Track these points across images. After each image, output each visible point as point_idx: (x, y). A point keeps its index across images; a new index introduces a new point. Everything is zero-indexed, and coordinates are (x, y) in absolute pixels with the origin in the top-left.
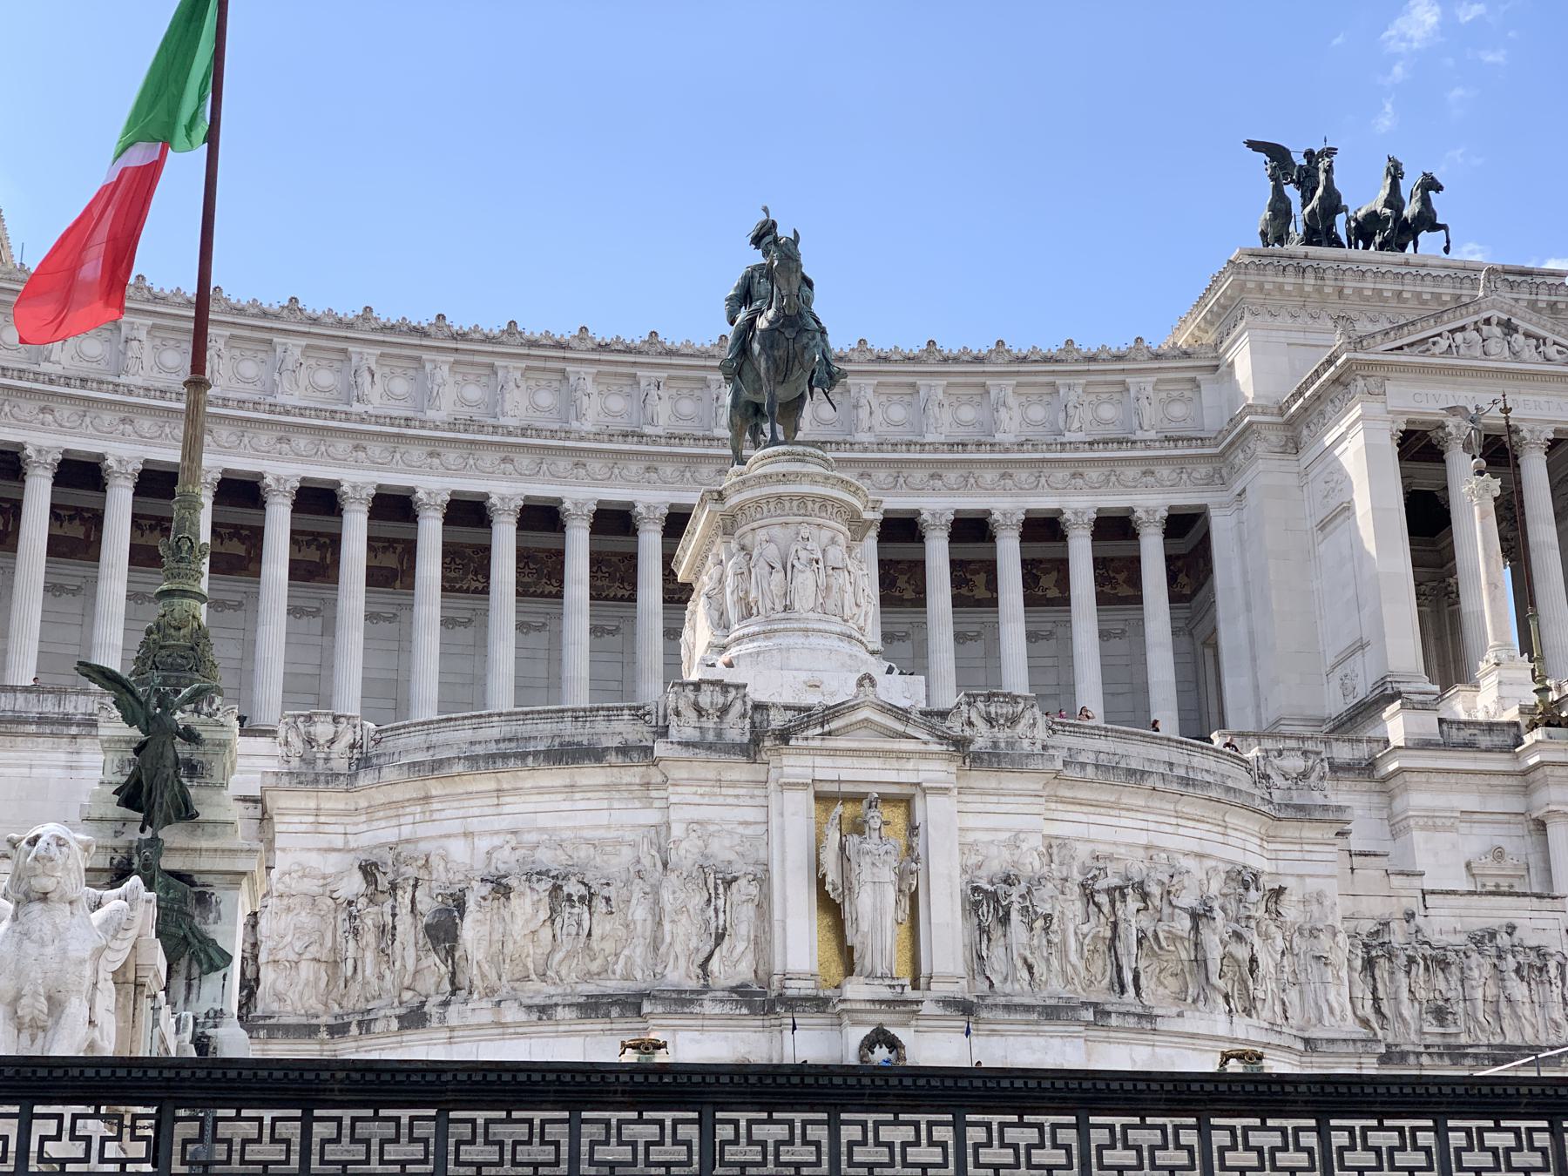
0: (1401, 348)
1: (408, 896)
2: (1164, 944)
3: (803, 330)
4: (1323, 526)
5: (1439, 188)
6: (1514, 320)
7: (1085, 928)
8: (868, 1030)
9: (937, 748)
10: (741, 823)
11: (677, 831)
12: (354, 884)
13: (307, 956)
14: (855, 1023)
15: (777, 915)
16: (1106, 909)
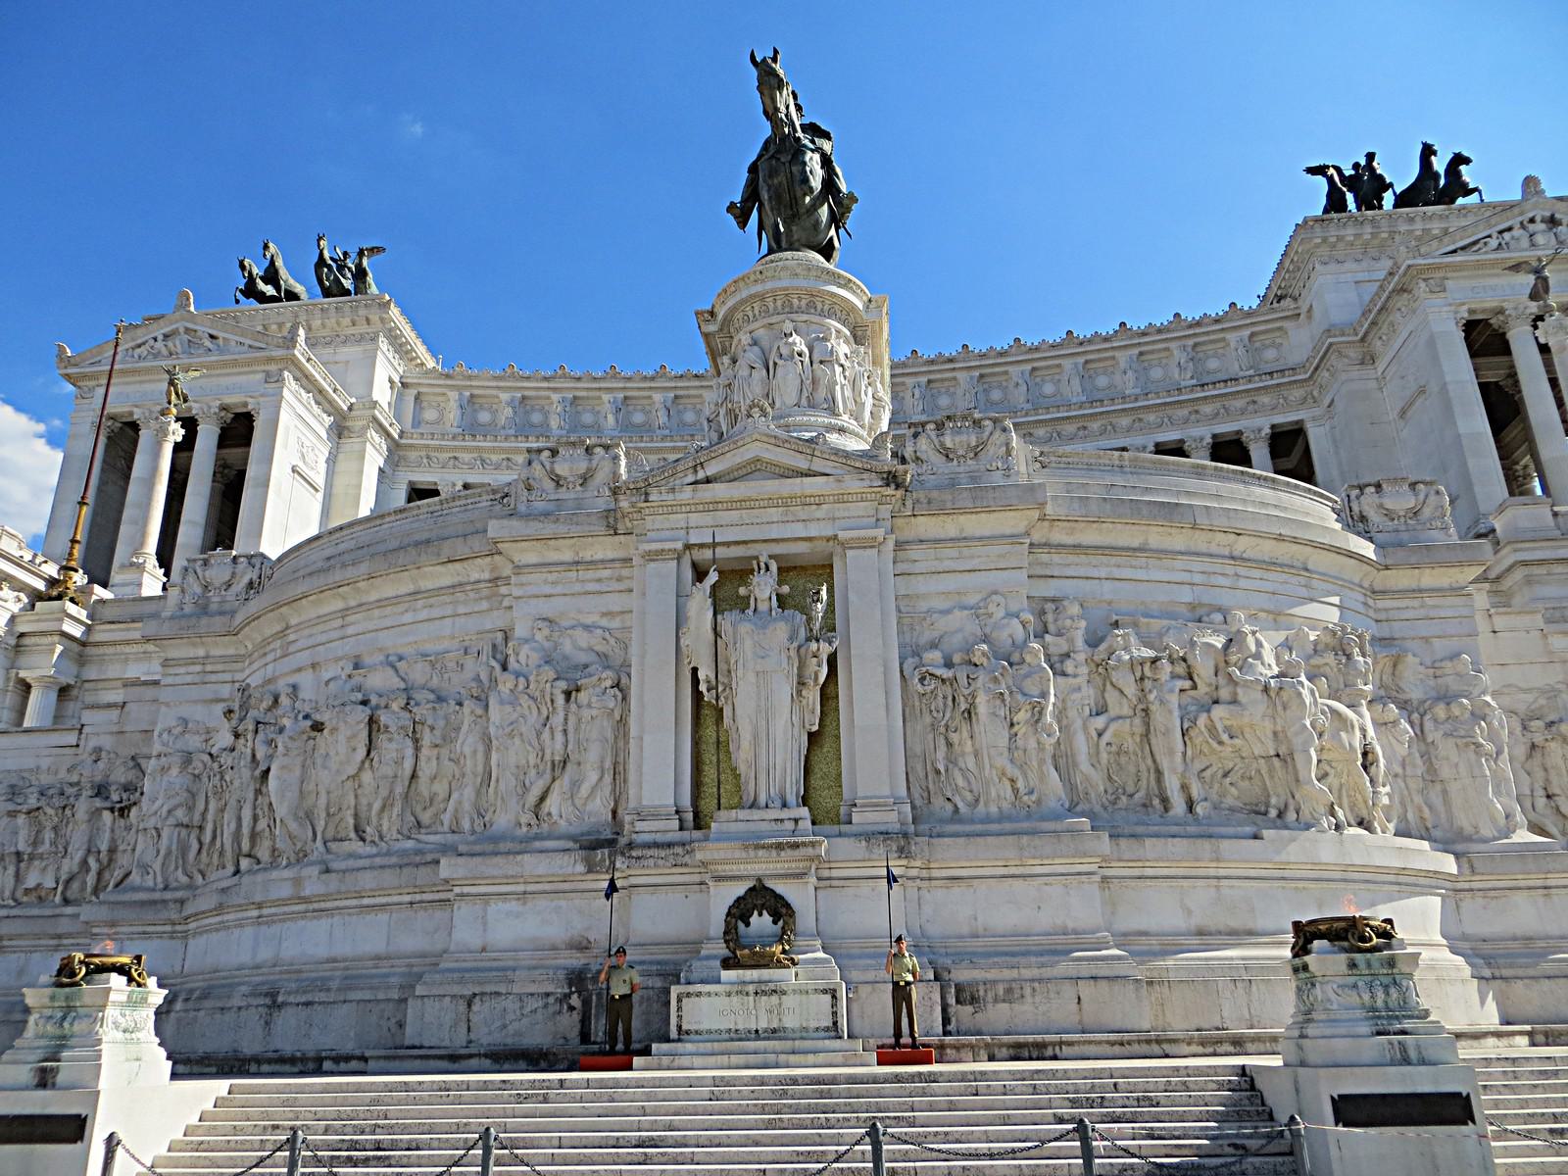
0: (1455, 251)
1: (250, 744)
2: (1225, 737)
3: (799, 150)
4: (1403, 413)
5: (1467, 161)
6: (1557, 216)
7: (1099, 722)
8: (740, 889)
9: (854, 484)
10: (604, 614)
11: (520, 631)
12: (227, 739)
13: (171, 821)
14: (719, 879)
15: (633, 732)
16: (1131, 690)
